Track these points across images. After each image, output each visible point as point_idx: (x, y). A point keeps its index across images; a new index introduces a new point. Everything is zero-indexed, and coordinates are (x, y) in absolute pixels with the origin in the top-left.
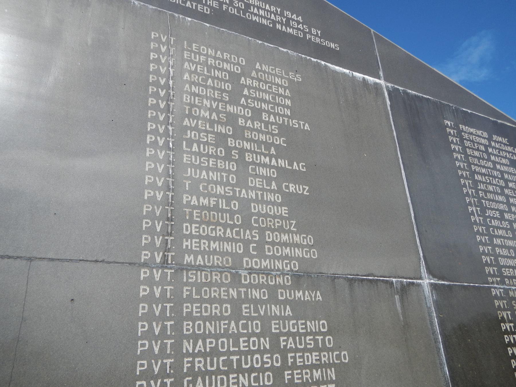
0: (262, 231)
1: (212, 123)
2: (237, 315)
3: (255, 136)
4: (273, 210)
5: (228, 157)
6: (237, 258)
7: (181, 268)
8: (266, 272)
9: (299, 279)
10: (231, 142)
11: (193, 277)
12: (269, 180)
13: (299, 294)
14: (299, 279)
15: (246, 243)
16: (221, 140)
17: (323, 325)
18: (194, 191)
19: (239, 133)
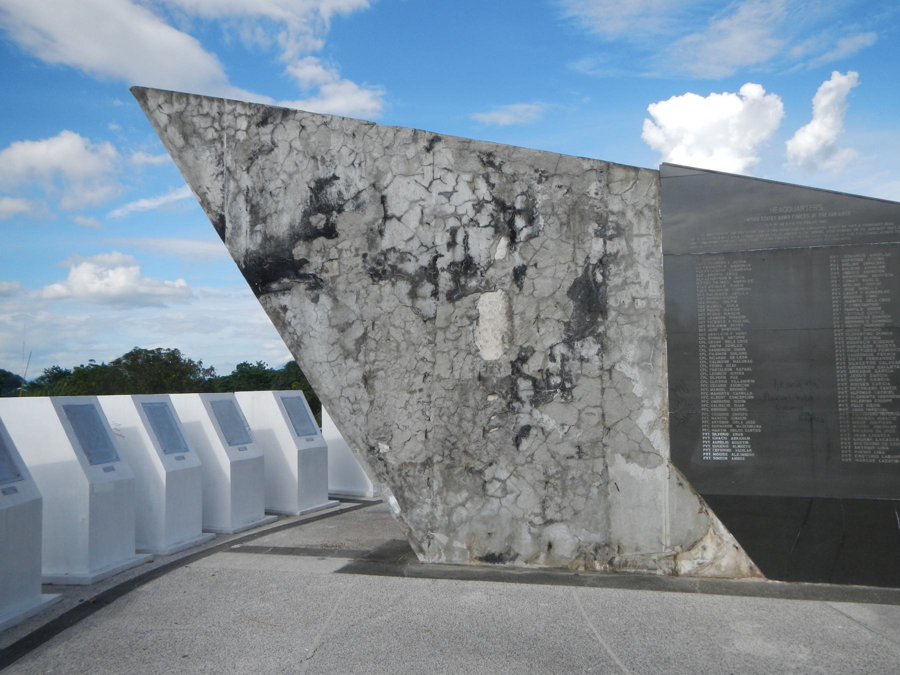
0: (871, 316)
1: (852, 283)
2: (862, 340)
3: (869, 284)
4: (875, 309)
5: (859, 294)
6: (862, 324)
7: (845, 328)
8: (872, 328)
9: (883, 329)
10: (860, 289)
11: (849, 331)
12: (874, 299)
13: (883, 333)
14: (883, 329)
15: (865, 320)
16: (856, 289)
17: (892, 341)
18: (848, 307)
19: (863, 285)
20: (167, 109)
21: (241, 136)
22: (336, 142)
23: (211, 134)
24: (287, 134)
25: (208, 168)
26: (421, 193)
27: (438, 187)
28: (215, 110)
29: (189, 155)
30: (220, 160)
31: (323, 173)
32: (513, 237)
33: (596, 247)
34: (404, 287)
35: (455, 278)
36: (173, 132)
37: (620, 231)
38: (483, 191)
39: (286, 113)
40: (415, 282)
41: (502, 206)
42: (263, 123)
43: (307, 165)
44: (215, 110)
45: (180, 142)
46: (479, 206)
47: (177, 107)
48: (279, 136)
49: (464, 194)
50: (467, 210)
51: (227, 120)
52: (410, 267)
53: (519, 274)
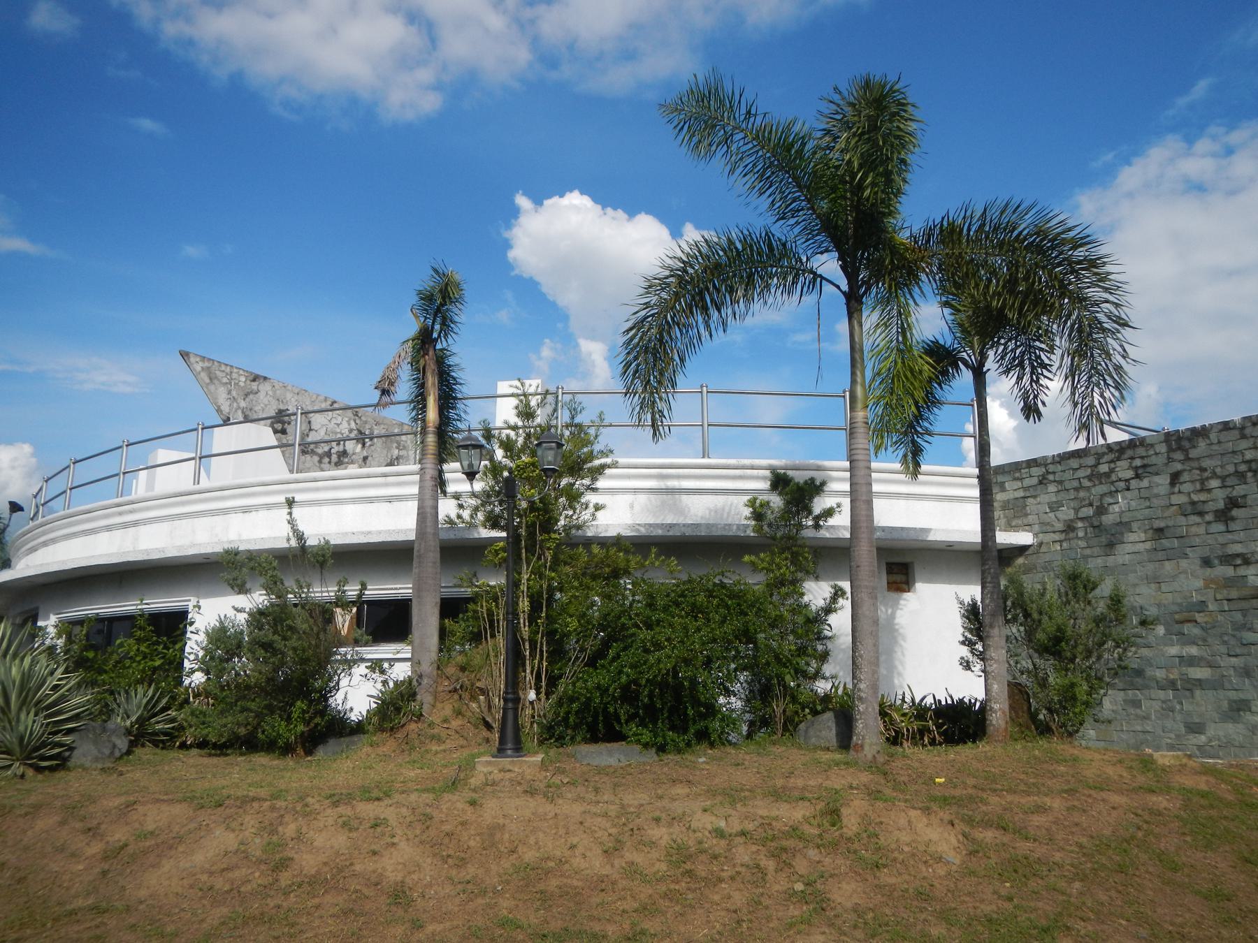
20: (201, 364)
21: (242, 384)
22: (289, 396)
23: (225, 380)
24: (265, 388)
25: (222, 394)
26: (326, 422)
27: (334, 421)
28: (228, 369)
29: (212, 388)
30: (229, 392)
31: (282, 407)
32: (364, 445)
33: (396, 452)
34: (316, 458)
35: (339, 457)
36: (204, 376)
37: (404, 448)
38: (353, 425)
39: (265, 378)
40: (321, 457)
41: (360, 432)
42: (254, 380)
43: (274, 403)
44: (228, 369)
45: (208, 381)
46: (351, 431)
47: (207, 364)
48: (261, 387)
49: (345, 425)
50: (346, 432)
51: (234, 376)
52: (320, 451)
53: (365, 459)
